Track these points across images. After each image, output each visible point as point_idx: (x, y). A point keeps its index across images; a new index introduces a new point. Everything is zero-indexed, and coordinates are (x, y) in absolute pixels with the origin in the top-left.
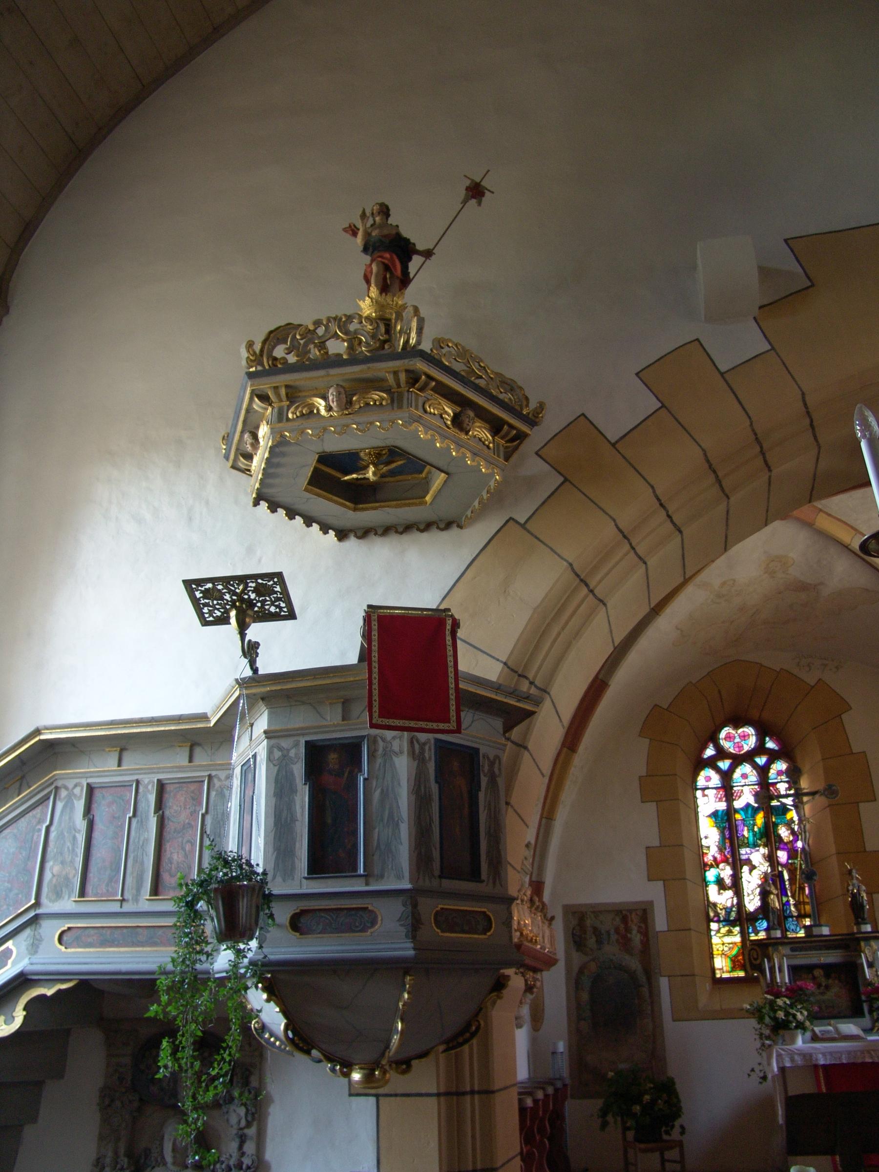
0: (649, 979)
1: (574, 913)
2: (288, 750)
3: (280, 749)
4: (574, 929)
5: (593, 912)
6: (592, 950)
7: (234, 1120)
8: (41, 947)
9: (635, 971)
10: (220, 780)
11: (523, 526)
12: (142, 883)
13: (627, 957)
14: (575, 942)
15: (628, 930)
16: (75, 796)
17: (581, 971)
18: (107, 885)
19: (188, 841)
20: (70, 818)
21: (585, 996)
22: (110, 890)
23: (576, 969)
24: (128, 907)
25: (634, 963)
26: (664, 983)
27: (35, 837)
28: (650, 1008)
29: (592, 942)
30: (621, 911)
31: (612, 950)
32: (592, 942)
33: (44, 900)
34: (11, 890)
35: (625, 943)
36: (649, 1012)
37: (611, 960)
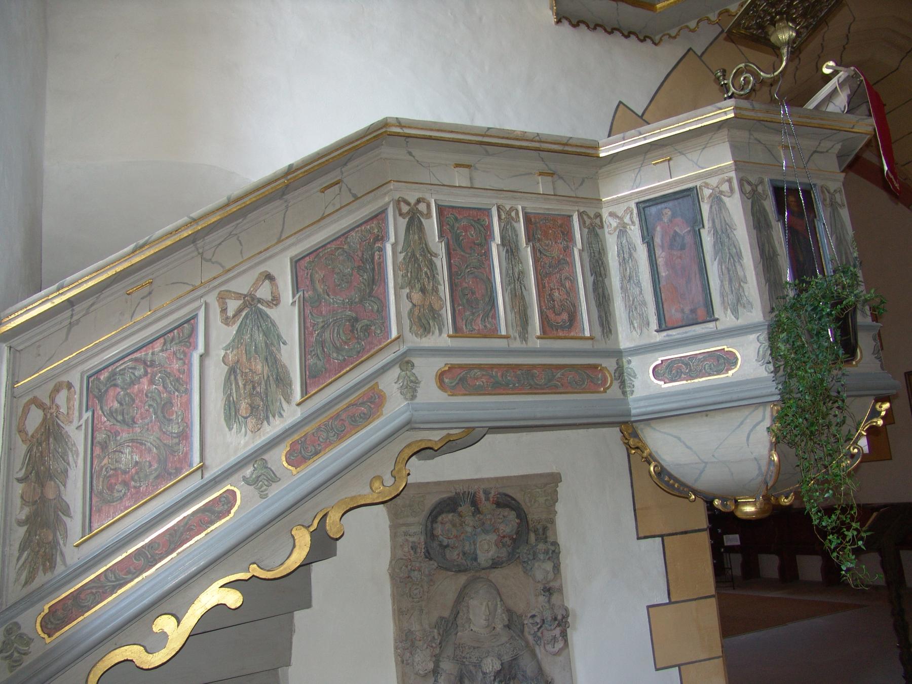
2: (756, 186)
3: (749, 183)
7: (539, 575)
8: (420, 391)
10: (589, 217)
11: (700, 57)
12: (527, 321)
16: (421, 213)
18: (483, 320)
19: (567, 278)
20: (420, 238)
22: (489, 326)
24: (517, 344)
27: (376, 257)
33: (408, 335)
34: (356, 320)
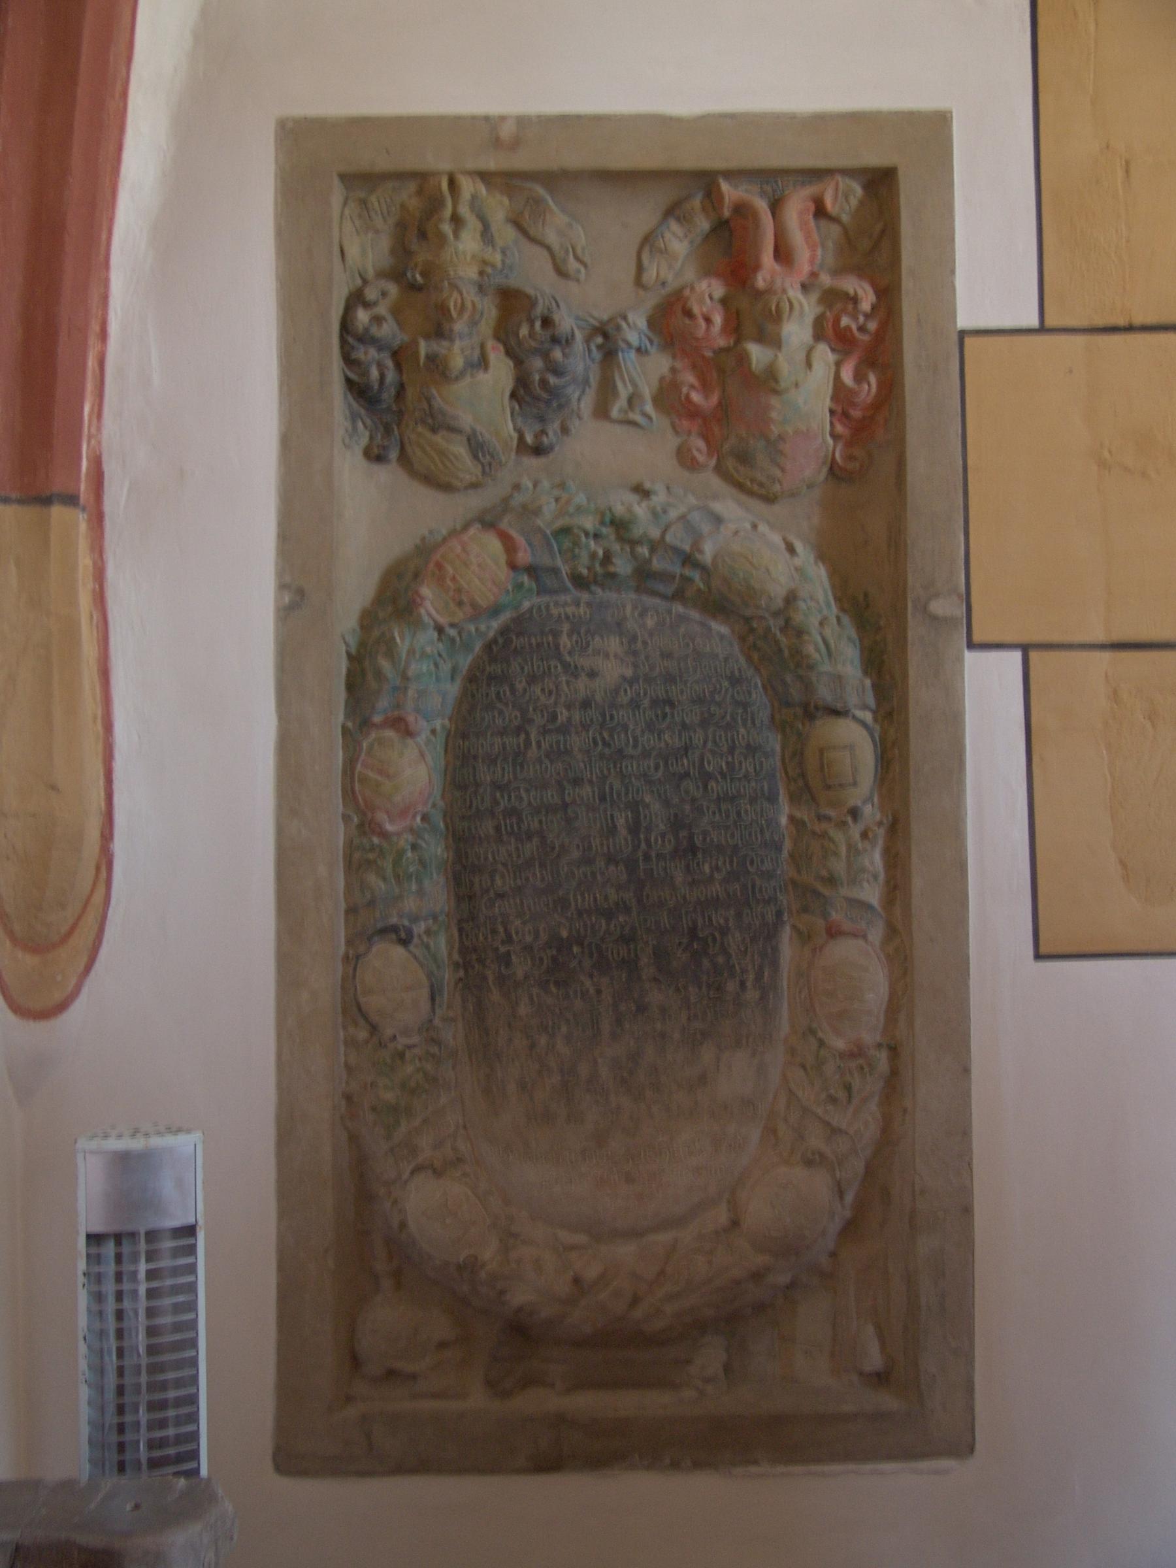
0: (884, 666)
1: (361, 182)
4: (356, 299)
5: (504, 180)
6: (476, 446)
9: (791, 598)
13: (732, 508)
14: (359, 390)
15: (751, 316)
17: (395, 597)
21: (414, 771)
23: (354, 589)
25: (776, 551)
26: (989, 686)
28: (875, 859)
29: (481, 395)
30: (706, 182)
31: (621, 460)
32: (481, 395)
35: (723, 413)
36: (872, 894)
37: (620, 526)
